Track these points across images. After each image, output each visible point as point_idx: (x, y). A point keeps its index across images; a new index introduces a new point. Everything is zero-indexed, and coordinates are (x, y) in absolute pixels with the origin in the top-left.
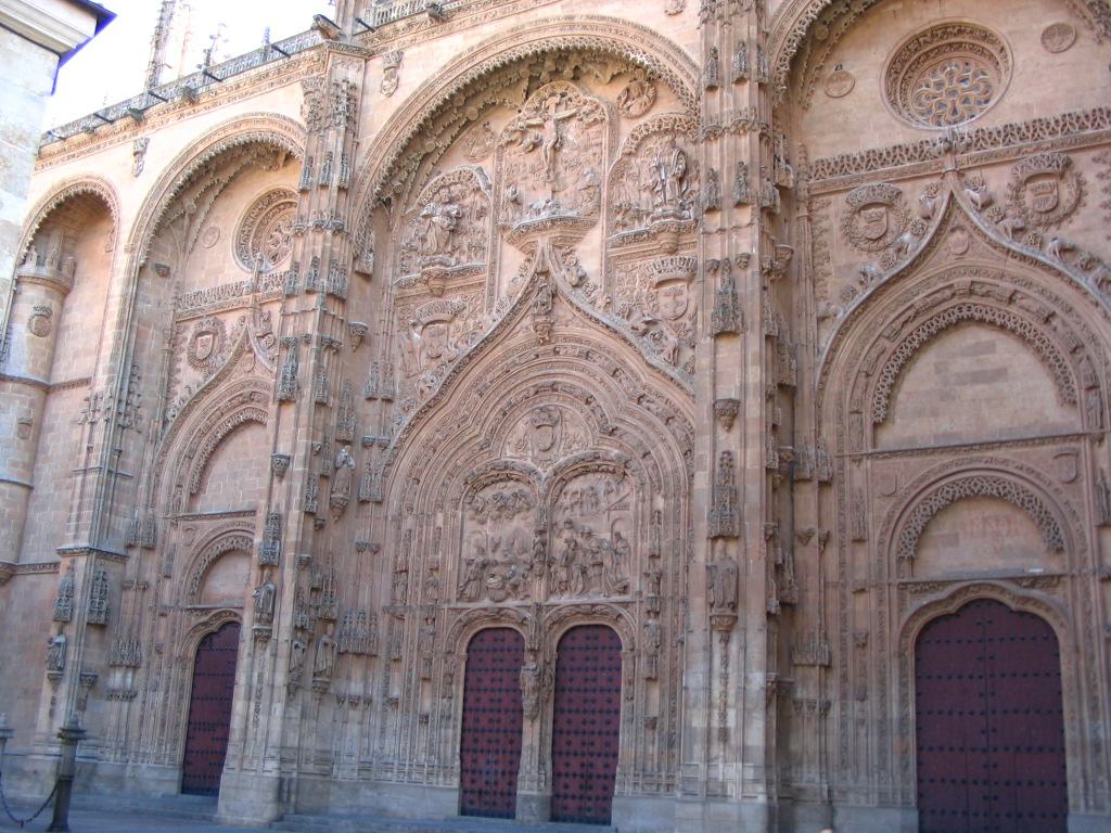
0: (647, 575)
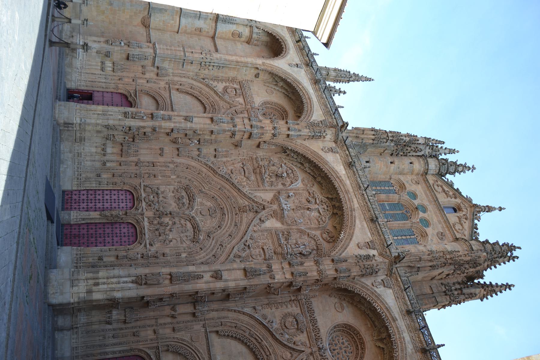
0: (157, 252)
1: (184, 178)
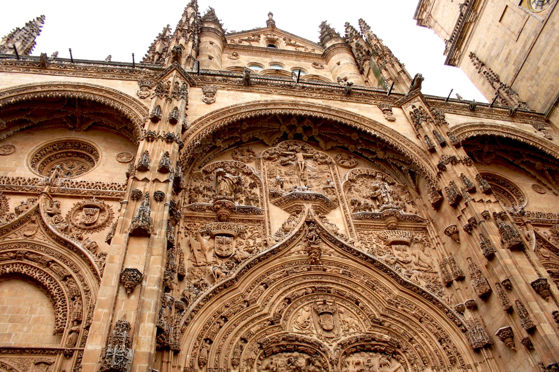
1: (239, 350)
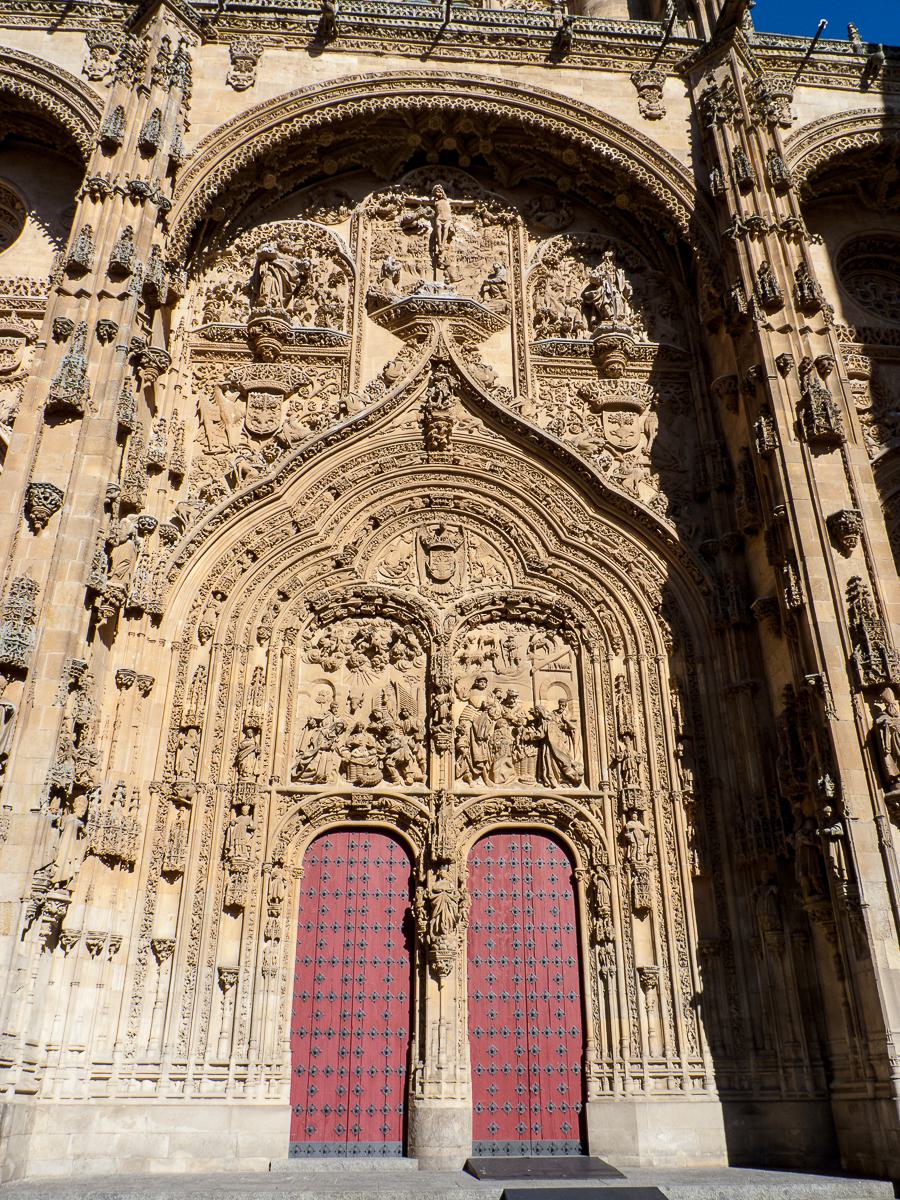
1: (272, 613)
